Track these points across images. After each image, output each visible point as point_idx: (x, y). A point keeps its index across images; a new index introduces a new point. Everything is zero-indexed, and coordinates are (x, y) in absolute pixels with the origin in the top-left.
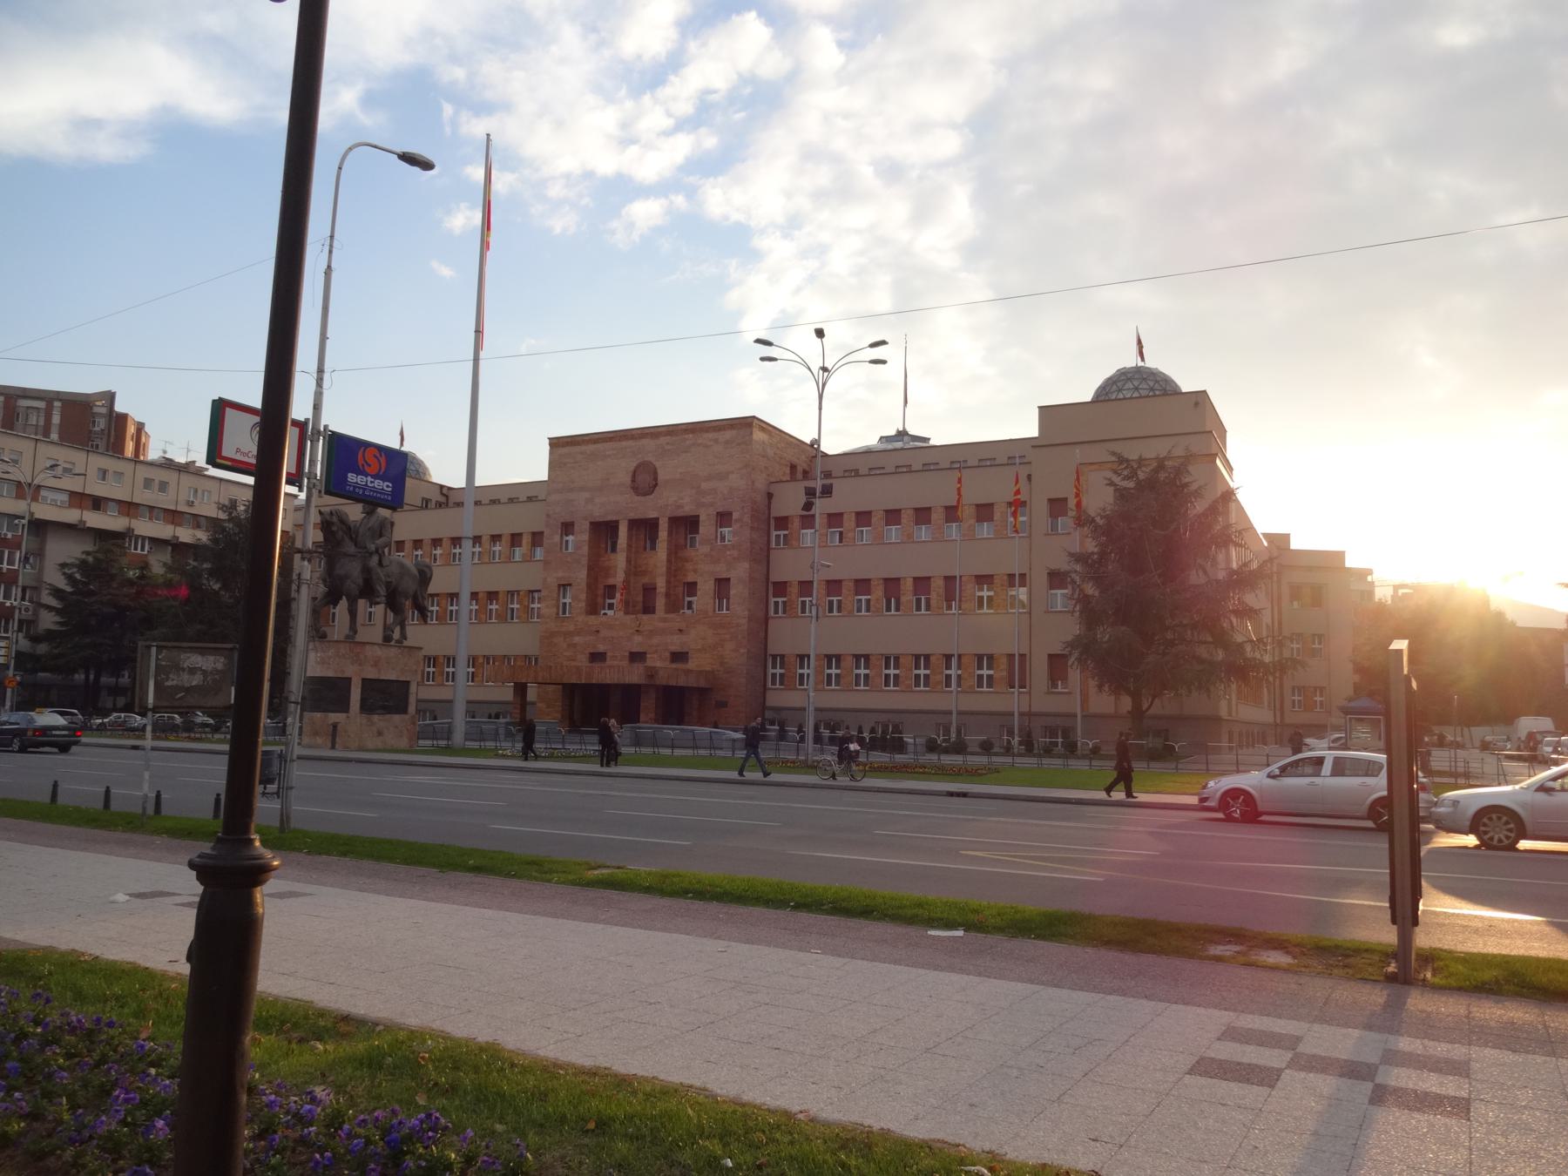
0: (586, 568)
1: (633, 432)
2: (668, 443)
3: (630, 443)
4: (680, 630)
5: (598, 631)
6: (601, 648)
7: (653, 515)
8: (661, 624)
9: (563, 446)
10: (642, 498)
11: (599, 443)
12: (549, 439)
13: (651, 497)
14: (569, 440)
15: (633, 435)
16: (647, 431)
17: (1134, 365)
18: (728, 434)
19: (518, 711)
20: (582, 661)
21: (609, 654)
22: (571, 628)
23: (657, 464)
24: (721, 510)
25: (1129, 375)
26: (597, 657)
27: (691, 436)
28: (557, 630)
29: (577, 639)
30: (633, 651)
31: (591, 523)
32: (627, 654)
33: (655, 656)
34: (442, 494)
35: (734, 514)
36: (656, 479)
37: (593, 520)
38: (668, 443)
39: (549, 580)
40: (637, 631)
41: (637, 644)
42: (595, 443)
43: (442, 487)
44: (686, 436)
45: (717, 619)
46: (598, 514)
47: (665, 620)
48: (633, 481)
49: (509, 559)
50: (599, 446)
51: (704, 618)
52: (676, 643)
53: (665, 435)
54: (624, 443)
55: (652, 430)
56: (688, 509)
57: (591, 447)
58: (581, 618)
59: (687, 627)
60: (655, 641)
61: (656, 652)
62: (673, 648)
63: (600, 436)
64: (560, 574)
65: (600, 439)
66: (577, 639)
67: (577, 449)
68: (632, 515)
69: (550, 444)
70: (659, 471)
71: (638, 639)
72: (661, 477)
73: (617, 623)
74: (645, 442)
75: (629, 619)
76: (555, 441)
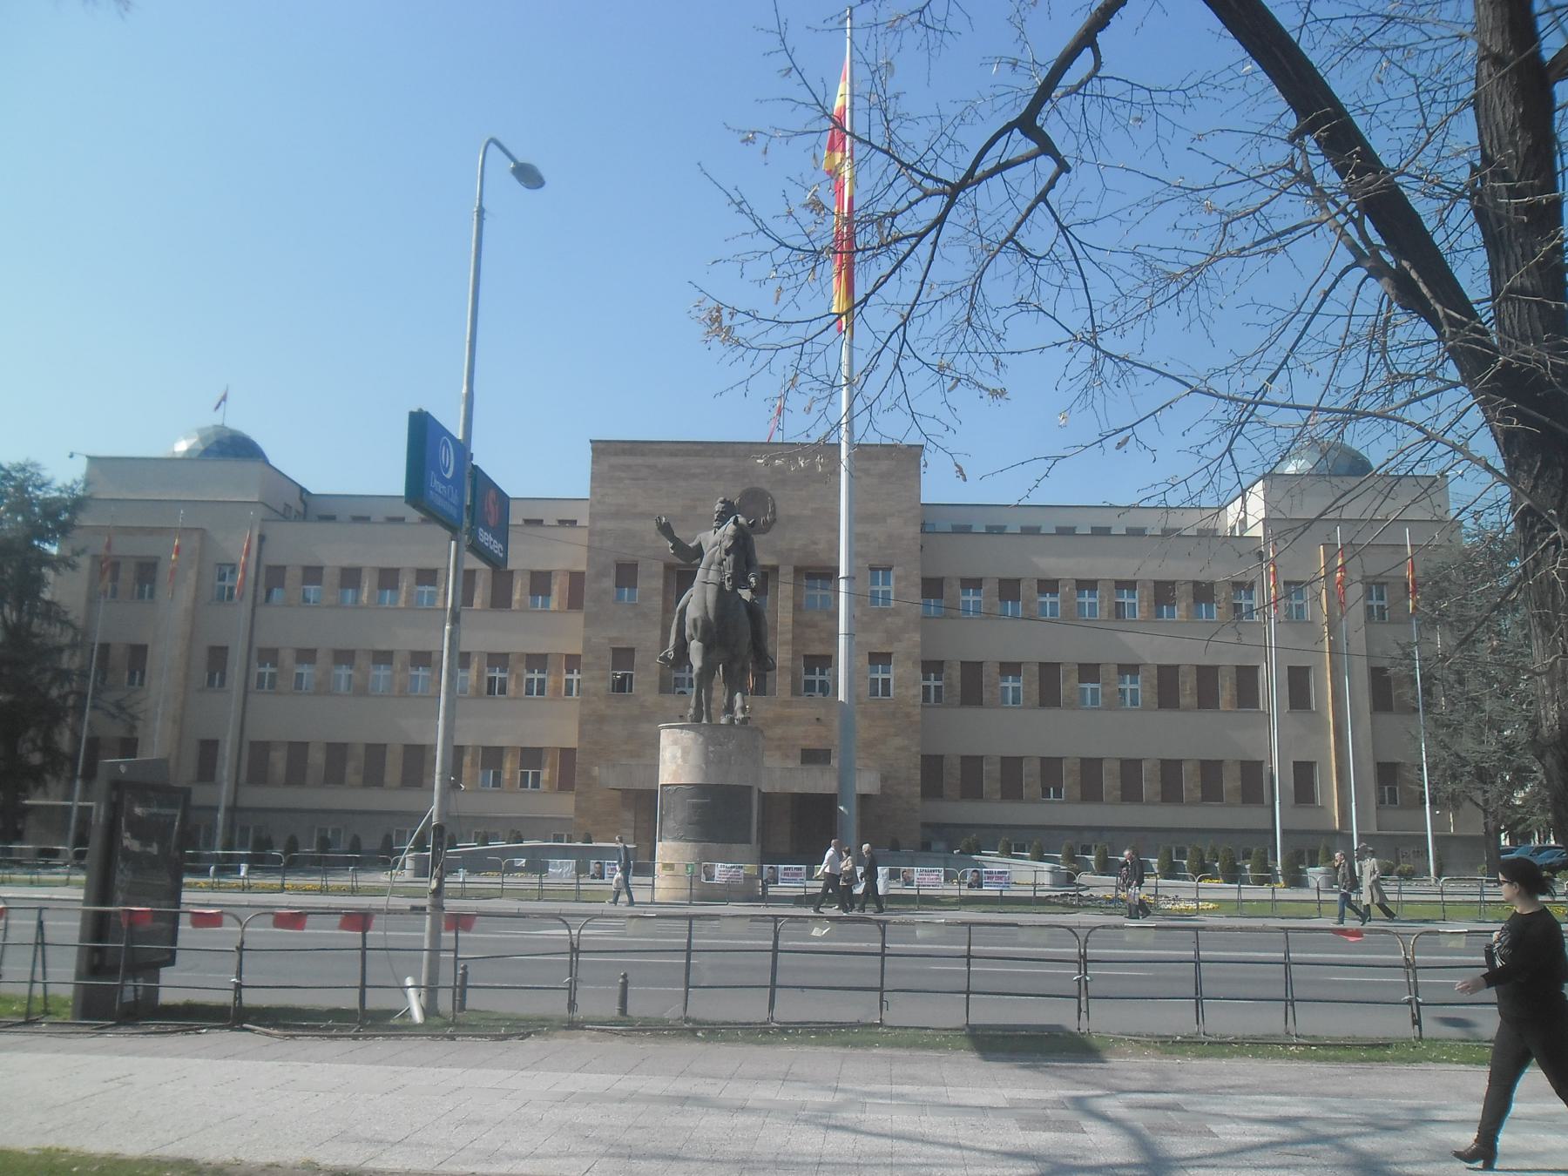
0: (660, 626)
3: (728, 461)
9: (616, 454)
11: (676, 455)
12: (591, 441)
14: (627, 446)
34: (301, 499)
43: (303, 490)
50: (678, 460)
54: (719, 461)
57: (666, 461)
63: (679, 447)
67: (639, 460)
69: (593, 450)
70: (778, 503)
76: (601, 446)
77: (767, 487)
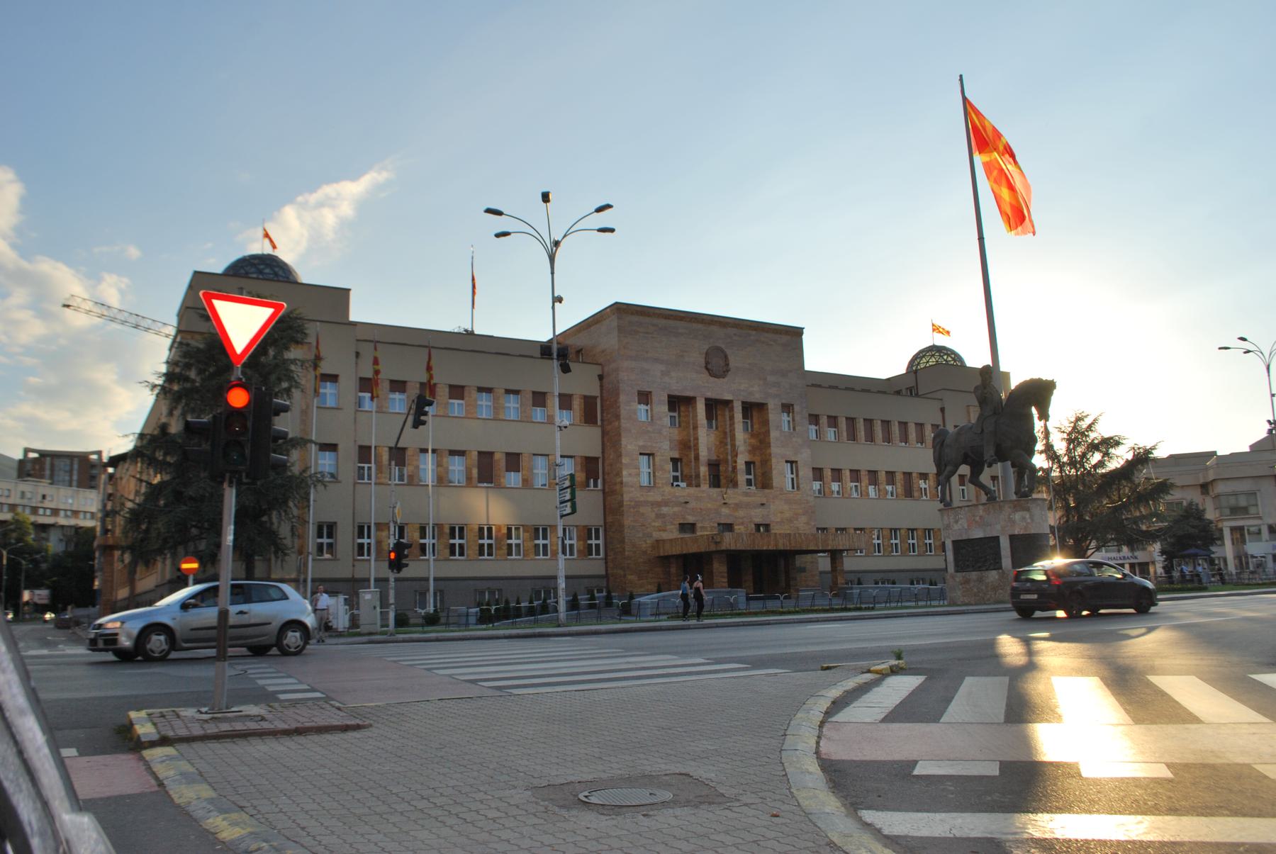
1: (705, 317)
2: (735, 334)
3: (700, 326)
4: (763, 504)
5: (687, 503)
6: (691, 519)
7: (728, 397)
8: (745, 499)
9: (632, 314)
10: (716, 379)
11: (669, 319)
13: (726, 380)
14: (639, 309)
15: (703, 320)
16: (716, 319)
17: (931, 344)
18: (785, 339)
19: (726, 580)
20: (672, 533)
21: (699, 525)
22: (659, 498)
23: (728, 352)
24: (784, 401)
25: (949, 352)
26: (688, 527)
27: (754, 332)
28: (642, 499)
29: (665, 510)
30: (723, 522)
31: (670, 397)
32: (716, 525)
33: (742, 527)
35: (795, 407)
36: (728, 365)
37: (671, 393)
38: (735, 334)
39: (629, 447)
40: (725, 503)
41: (726, 515)
42: (666, 318)
44: (750, 332)
45: (792, 495)
46: (675, 388)
47: (746, 494)
48: (707, 363)
49: (526, 420)
50: (671, 322)
51: (781, 494)
52: (758, 516)
53: (733, 327)
54: (695, 326)
55: (722, 320)
56: (757, 398)
57: (662, 322)
58: (668, 489)
59: (767, 502)
60: (741, 513)
61: (742, 524)
62: (758, 520)
63: (671, 313)
64: (641, 443)
65: (672, 316)
66: (665, 510)
68: (709, 395)
71: (725, 511)
72: (732, 364)
73: (705, 495)
74: (715, 328)
75: (715, 491)
77: (723, 346)
